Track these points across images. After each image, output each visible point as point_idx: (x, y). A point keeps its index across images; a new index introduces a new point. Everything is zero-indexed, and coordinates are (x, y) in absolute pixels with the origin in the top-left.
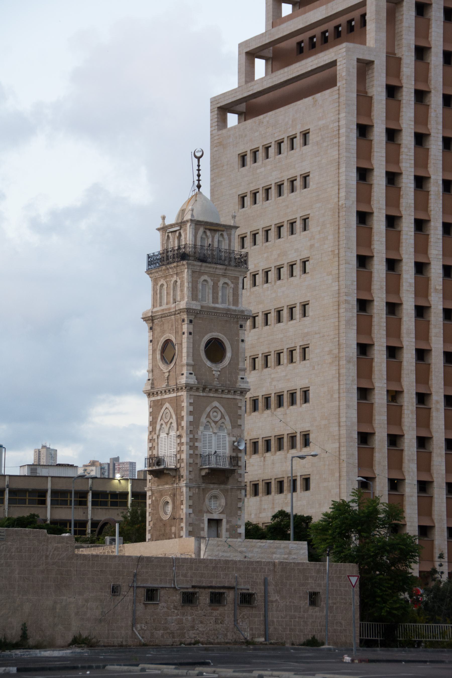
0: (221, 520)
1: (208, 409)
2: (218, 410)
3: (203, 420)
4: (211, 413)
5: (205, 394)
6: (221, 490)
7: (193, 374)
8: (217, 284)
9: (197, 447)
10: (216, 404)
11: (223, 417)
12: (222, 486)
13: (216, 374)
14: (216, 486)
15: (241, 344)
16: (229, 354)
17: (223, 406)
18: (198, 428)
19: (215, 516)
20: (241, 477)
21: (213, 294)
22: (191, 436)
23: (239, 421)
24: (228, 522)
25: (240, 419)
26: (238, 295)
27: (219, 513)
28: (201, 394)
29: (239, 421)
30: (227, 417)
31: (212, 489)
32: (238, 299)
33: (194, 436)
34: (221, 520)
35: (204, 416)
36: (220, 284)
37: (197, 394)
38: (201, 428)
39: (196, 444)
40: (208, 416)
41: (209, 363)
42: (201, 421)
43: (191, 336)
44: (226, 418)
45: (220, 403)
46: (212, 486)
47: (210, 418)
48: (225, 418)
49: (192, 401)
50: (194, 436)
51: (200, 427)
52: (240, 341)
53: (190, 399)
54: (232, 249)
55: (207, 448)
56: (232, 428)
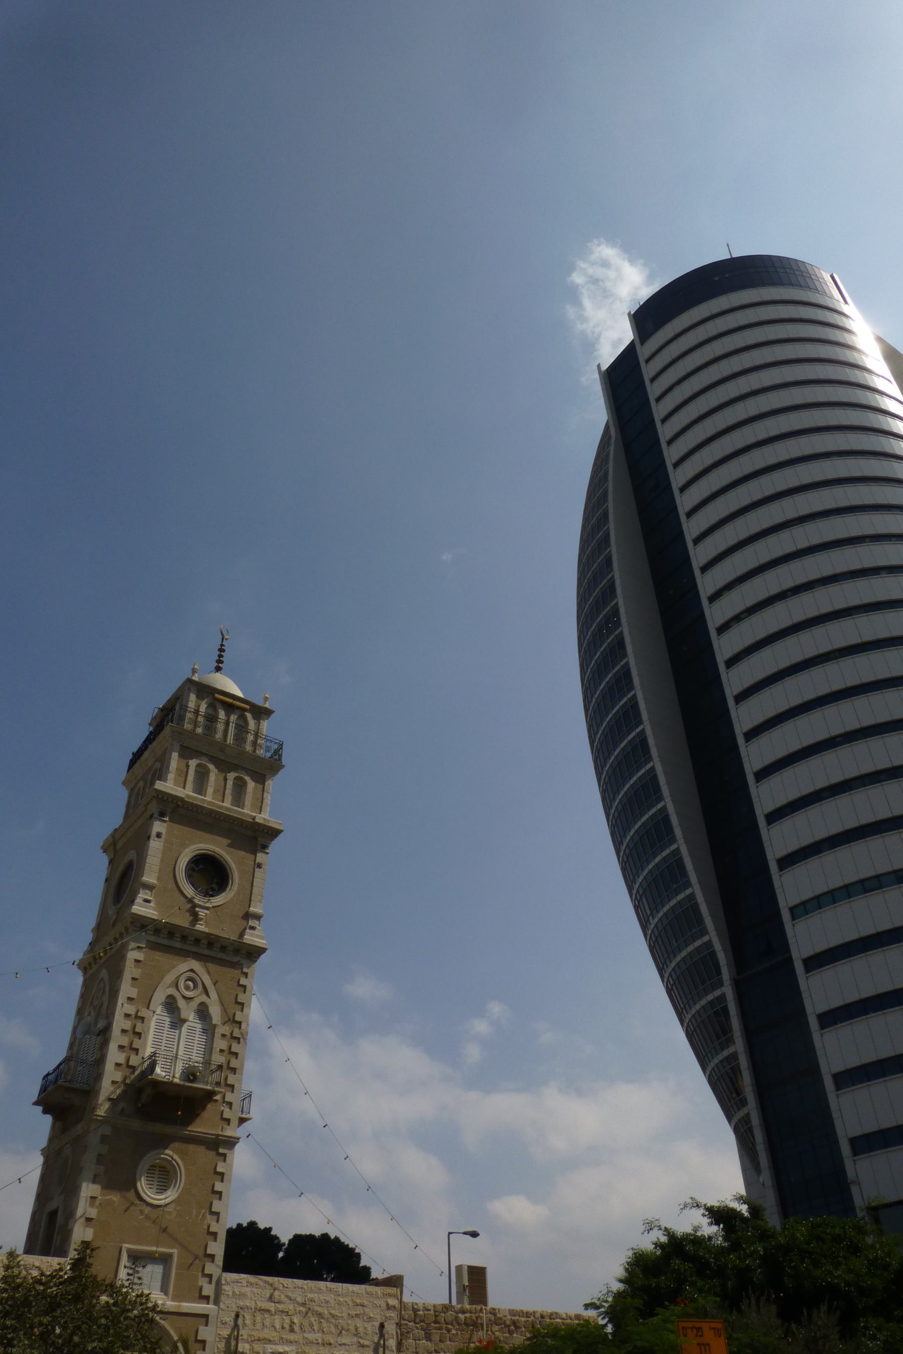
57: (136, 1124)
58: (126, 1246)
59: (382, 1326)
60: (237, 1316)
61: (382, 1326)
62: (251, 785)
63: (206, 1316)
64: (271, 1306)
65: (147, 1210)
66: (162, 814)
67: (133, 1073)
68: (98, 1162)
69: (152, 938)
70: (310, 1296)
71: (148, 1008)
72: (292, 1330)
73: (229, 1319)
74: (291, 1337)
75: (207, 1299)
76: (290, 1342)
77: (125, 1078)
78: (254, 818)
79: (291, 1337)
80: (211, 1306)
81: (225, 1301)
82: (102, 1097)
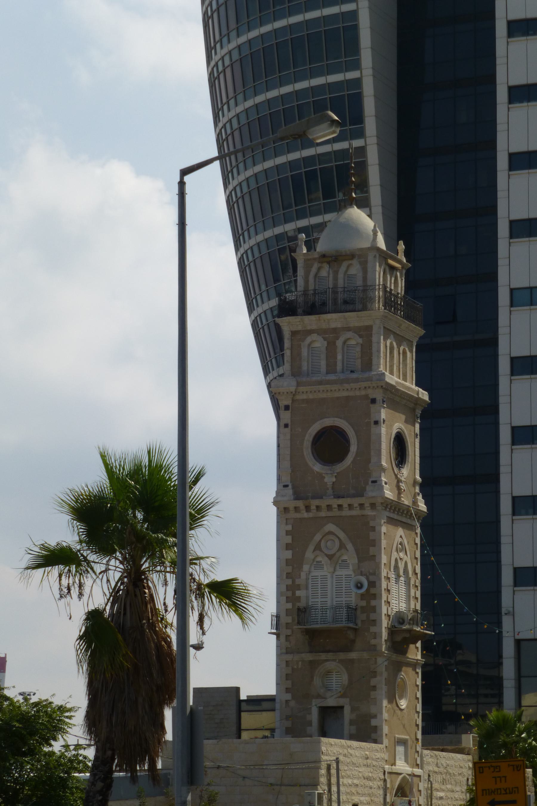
0: (342, 708)
1: (318, 537)
2: (331, 537)
3: (309, 554)
4: (323, 544)
5: (311, 515)
6: (341, 661)
7: (290, 487)
8: (334, 343)
9: (300, 597)
10: (331, 527)
11: (342, 546)
12: (342, 656)
13: (329, 480)
14: (330, 656)
15: (374, 428)
16: (353, 448)
17: (344, 531)
18: (300, 568)
19: (331, 702)
20: (375, 638)
21: (327, 360)
22: (289, 582)
23: (371, 549)
24: (353, 710)
25: (374, 546)
26: (371, 354)
27: (339, 697)
28: (306, 515)
29: (371, 549)
30: (350, 546)
31: (327, 660)
32: (371, 360)
33: (293, 582)
34: (342, 708)
35: (311, 547)
36: (339, 343)
37: (298, 516)
38: (306, 568)
39: (298, 593)
40: (318, 547)
41: (317, 467)
42: (306, 556)
43: (288, 430)
44: (348, 547)
45: (337, 526)
46: (323, 656)
47: (321, 550)
48: (346, 548)
49: (289, 528)
50: (293, 582)
51: (304, 566)
52: (372, 423)
53: (287, 524)
54: (369, 283)
55: (319, 597)
56: (359, 561)
57: (394, 657)
58: (397, 736)
59: (468, 780)
60: (429, 776)
61: (468, 780)
62: (409, 354)
63: (419, 776)
64: (436, 769)
65: (398, 712)
66: (383, 401)
67: (389, 620)
68: (386, 685)
69: (387, 513)
70: (448, 762)
71: (390, 571)
72: (443, 784)
73: (427, 778)
74: (443, 787)
75: (417, 765)
76: (443, 790)
77: (388, 624)
78: (418, 394)
79: (443, 787)
80: (420, 770)
81: (427, 768)
82: (383, 640)
